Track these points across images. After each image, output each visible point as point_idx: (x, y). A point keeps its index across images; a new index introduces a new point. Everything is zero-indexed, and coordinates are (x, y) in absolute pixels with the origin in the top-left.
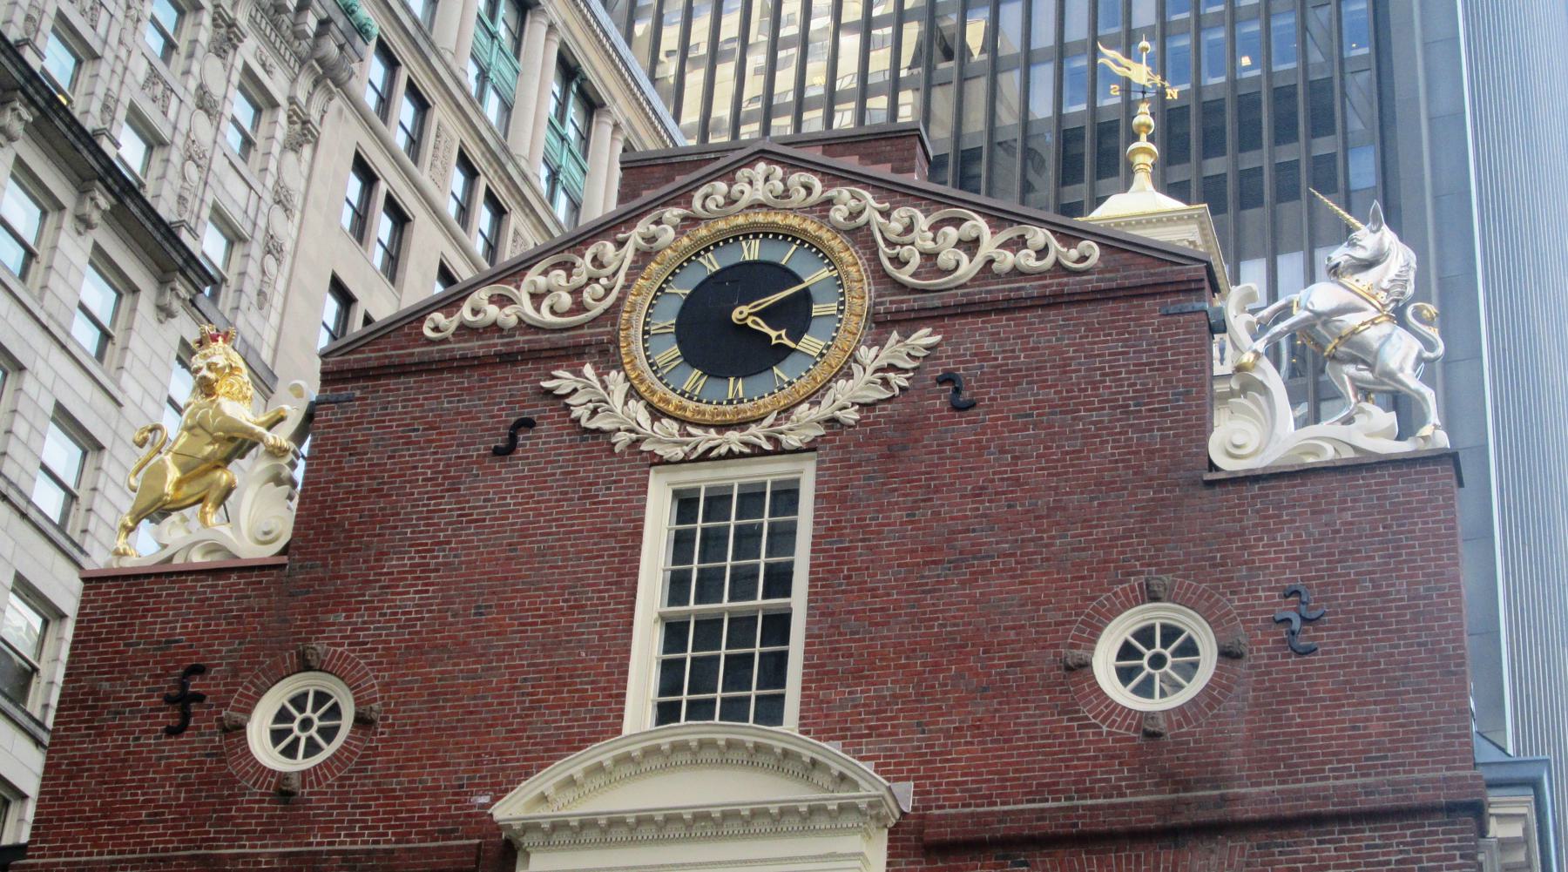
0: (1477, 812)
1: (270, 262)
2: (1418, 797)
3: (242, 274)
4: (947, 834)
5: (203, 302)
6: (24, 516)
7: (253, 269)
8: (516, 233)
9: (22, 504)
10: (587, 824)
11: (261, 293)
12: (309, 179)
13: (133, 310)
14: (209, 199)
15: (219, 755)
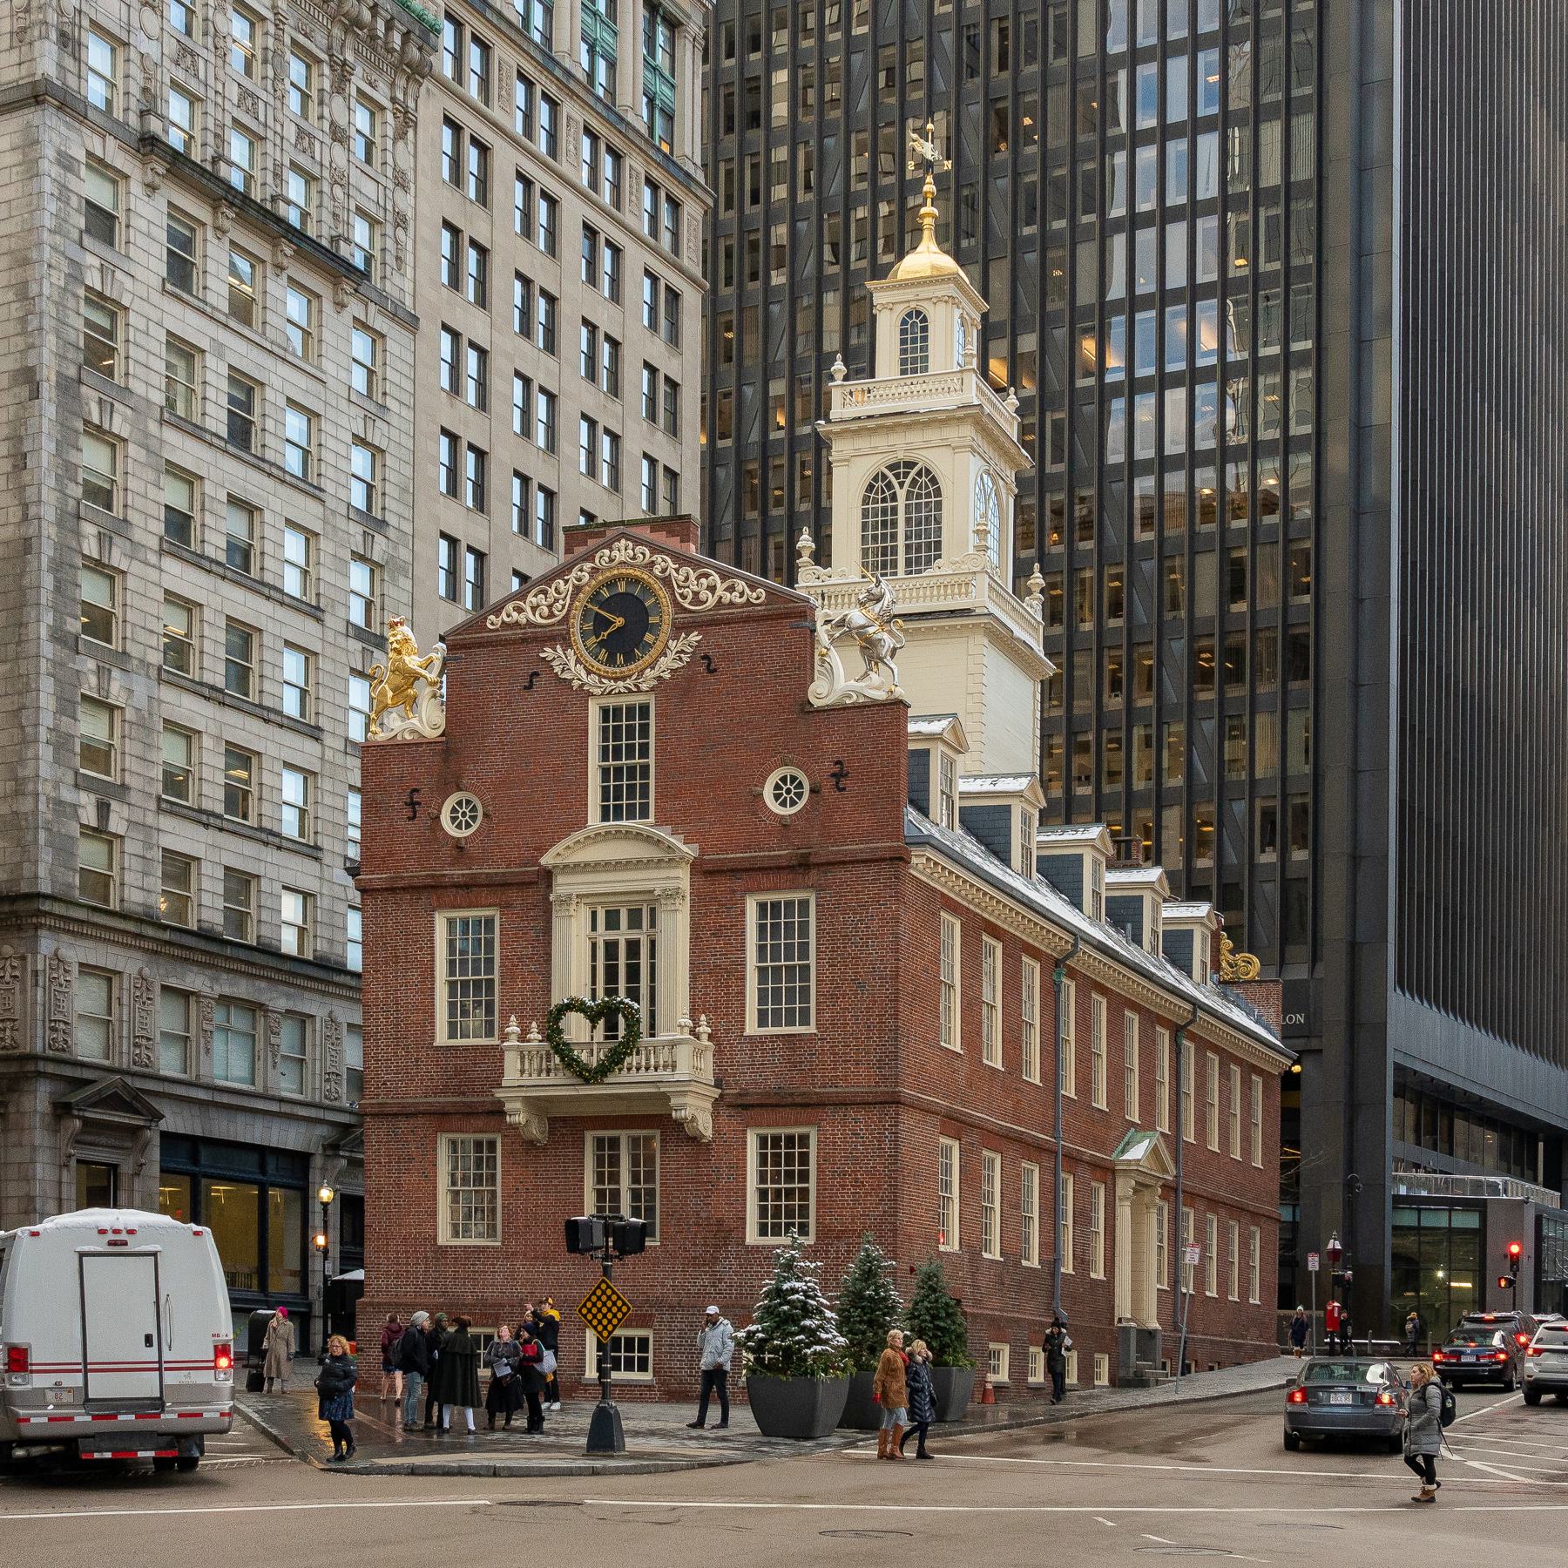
0: (901, 859)
1: (400, 232)
2: (879, 854)
3: (384, 250)
4: (710, 867)
5: (361, 289)
6: (283, 481)
7: (390, 244)
8: (569, 118)
9: (280, 474)
10: (577, 865)
11: (398, 258)
12: (415, 156)
13: (320, 311)
14: (353, 208)
15: (433, 830)
